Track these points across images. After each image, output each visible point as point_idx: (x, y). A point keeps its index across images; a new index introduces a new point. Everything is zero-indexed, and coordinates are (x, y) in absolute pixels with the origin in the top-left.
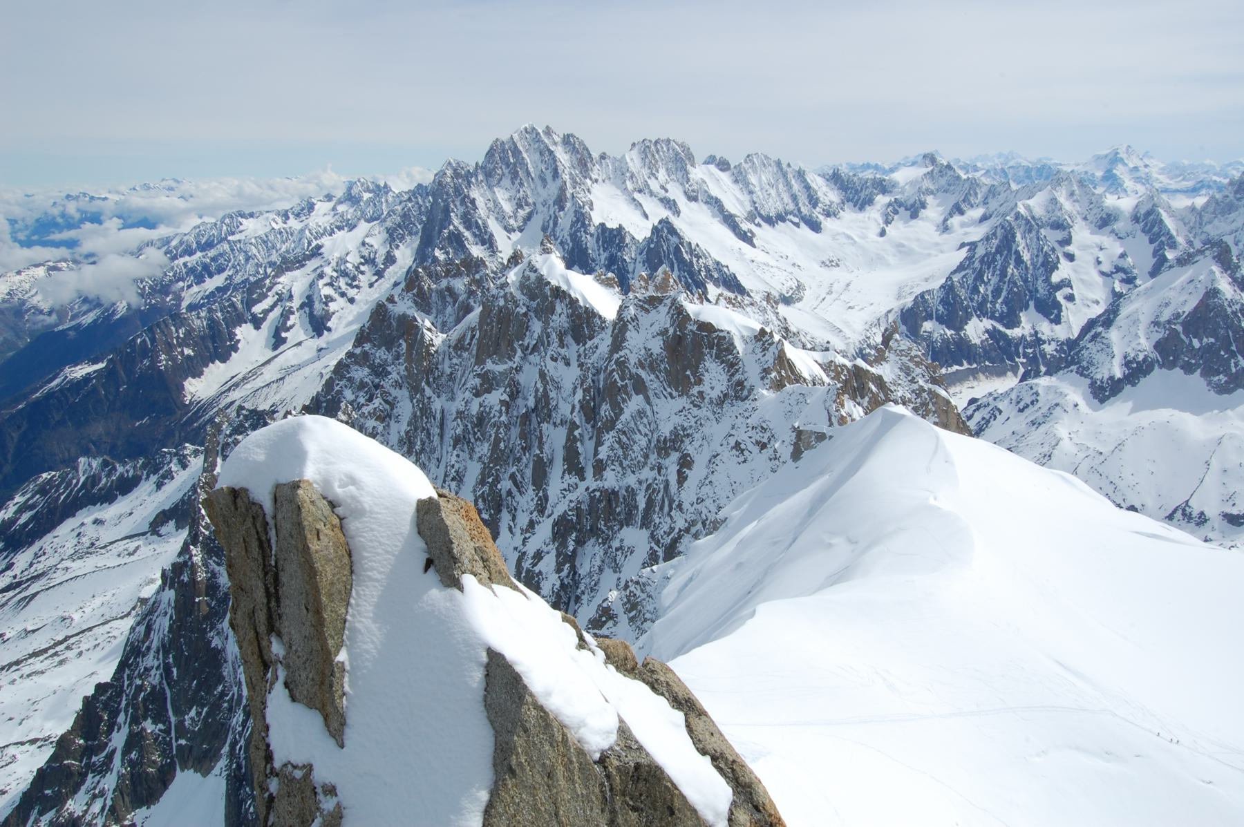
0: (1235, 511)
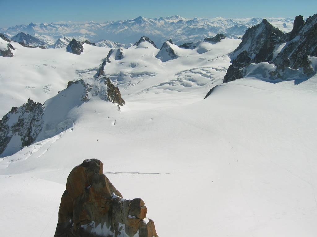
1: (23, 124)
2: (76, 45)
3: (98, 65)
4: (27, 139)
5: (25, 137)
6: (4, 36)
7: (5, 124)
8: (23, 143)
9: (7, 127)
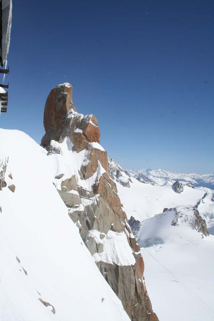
2: (178, 186)
3: (194, 204)
6: (127, 172)
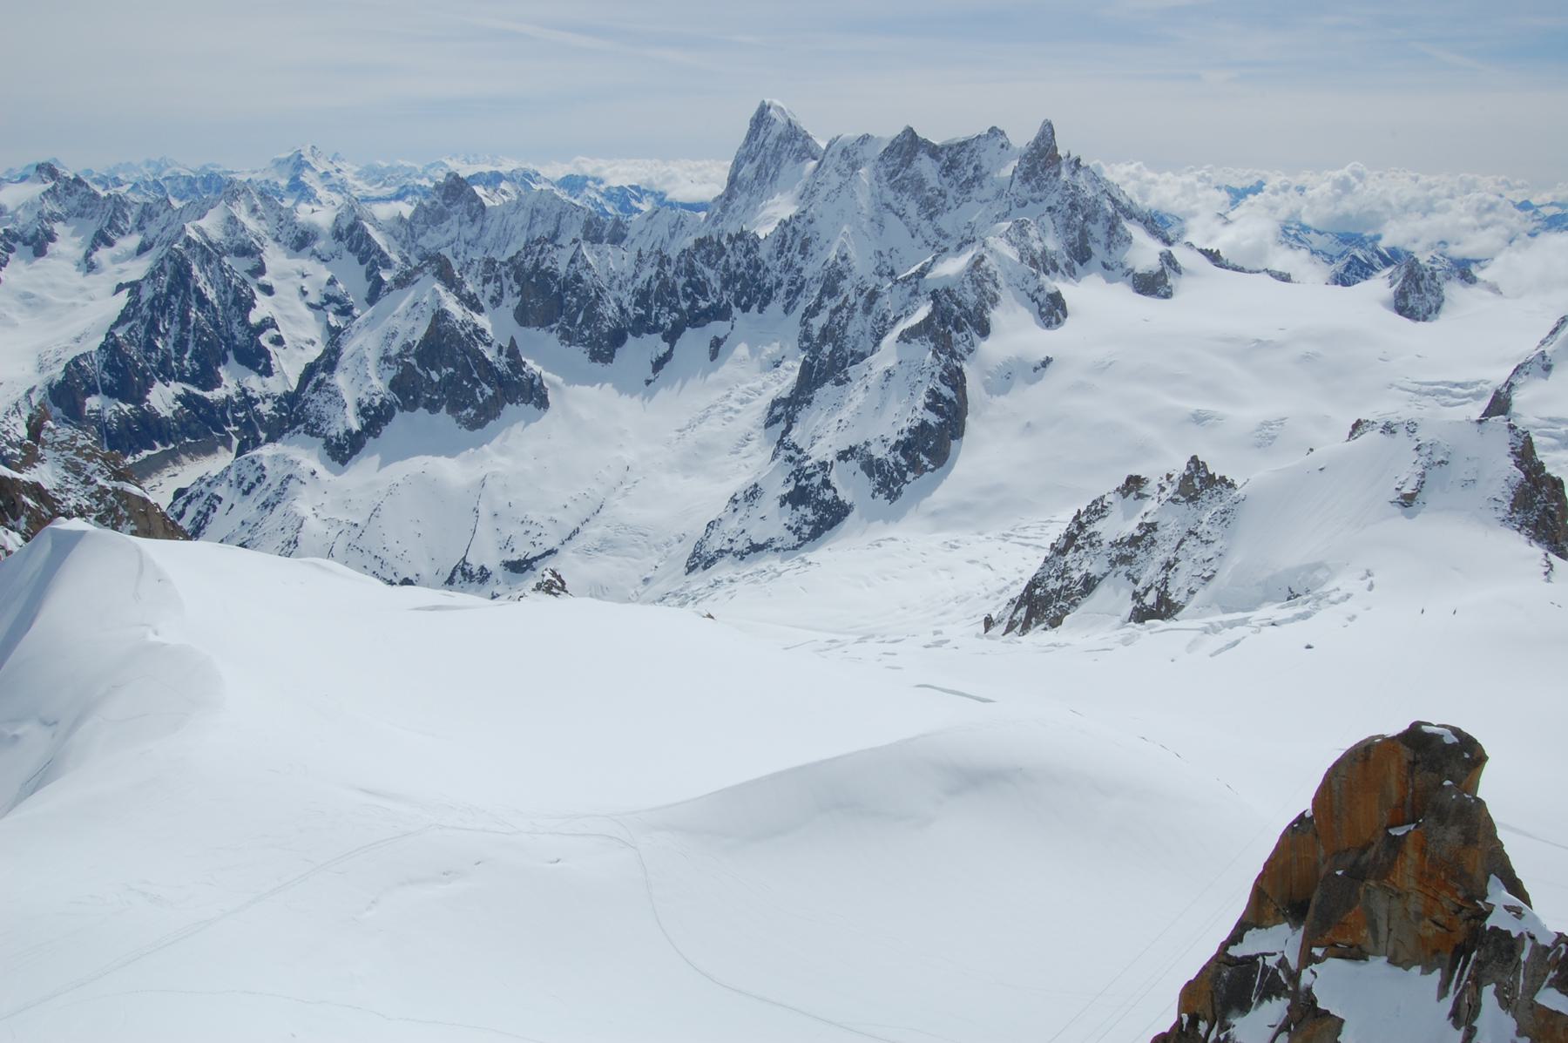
0: (515, 558)
1: (1153, 542)
4: (1150, 599)
5: (1147, 591)
7: (1090, 529)
8: (1135, 609)
9: (1093, 541)
